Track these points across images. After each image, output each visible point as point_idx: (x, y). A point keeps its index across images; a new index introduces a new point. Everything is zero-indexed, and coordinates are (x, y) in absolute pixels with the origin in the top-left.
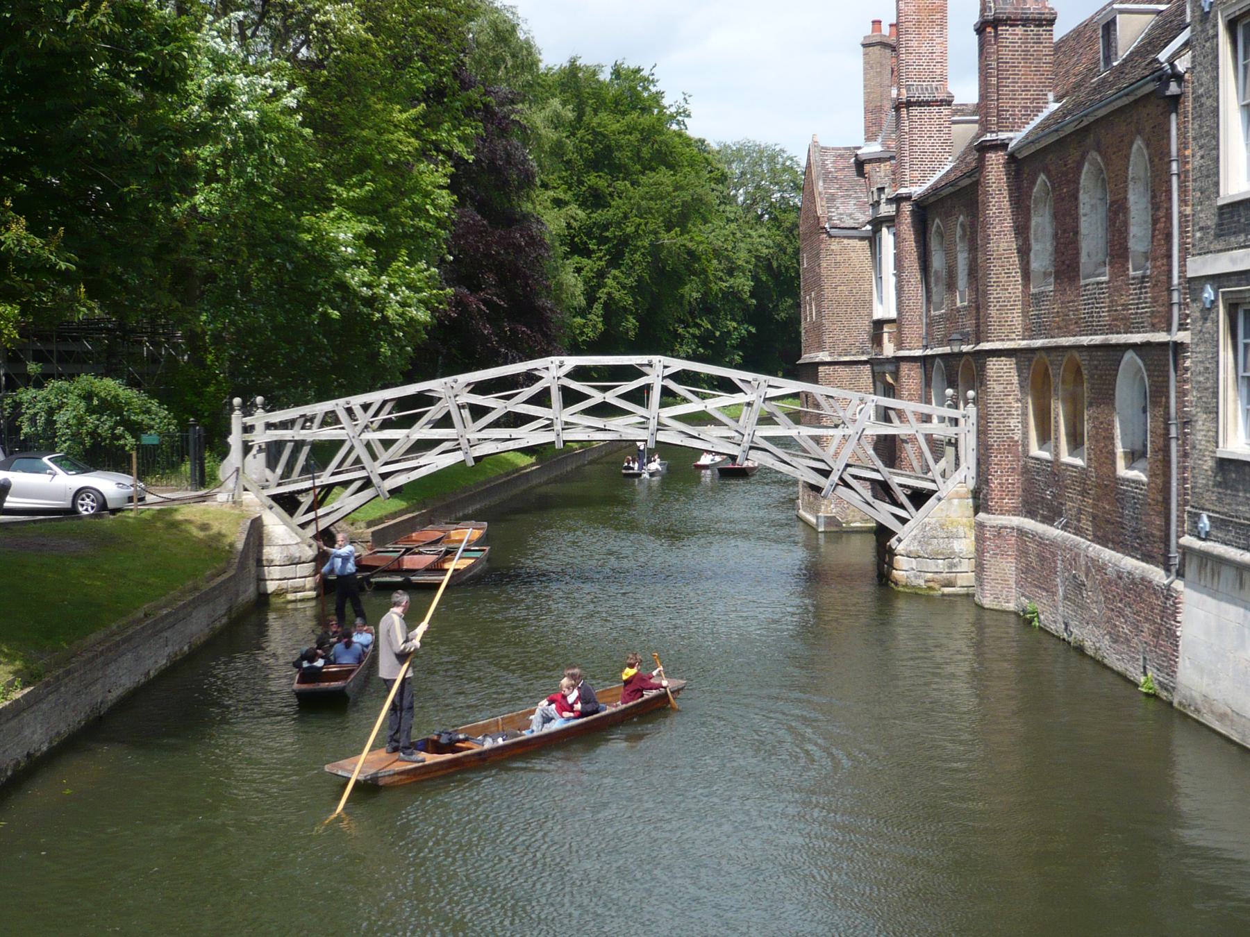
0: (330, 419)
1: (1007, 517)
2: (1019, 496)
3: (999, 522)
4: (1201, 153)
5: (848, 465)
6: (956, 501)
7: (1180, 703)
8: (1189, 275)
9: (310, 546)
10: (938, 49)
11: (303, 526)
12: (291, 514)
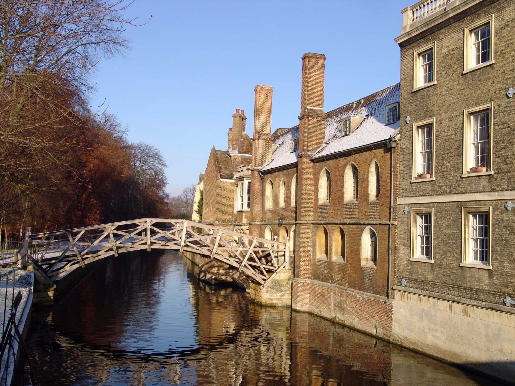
4: (404, 166)
7: (393, 340)
8: (398, 203)
10: (268, 122)
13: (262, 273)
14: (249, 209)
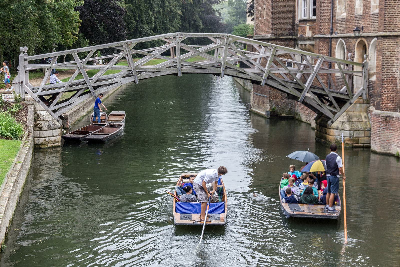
0: (61, 60)
1: (389, 112)
2: (396, 102)
3: (387, 114)
5: (311, 87)
6: (358, 105)
9: (58, 121)
11: (55, 111)
12: (49, 105)
13: (331, 104)
14: (315, 17)
